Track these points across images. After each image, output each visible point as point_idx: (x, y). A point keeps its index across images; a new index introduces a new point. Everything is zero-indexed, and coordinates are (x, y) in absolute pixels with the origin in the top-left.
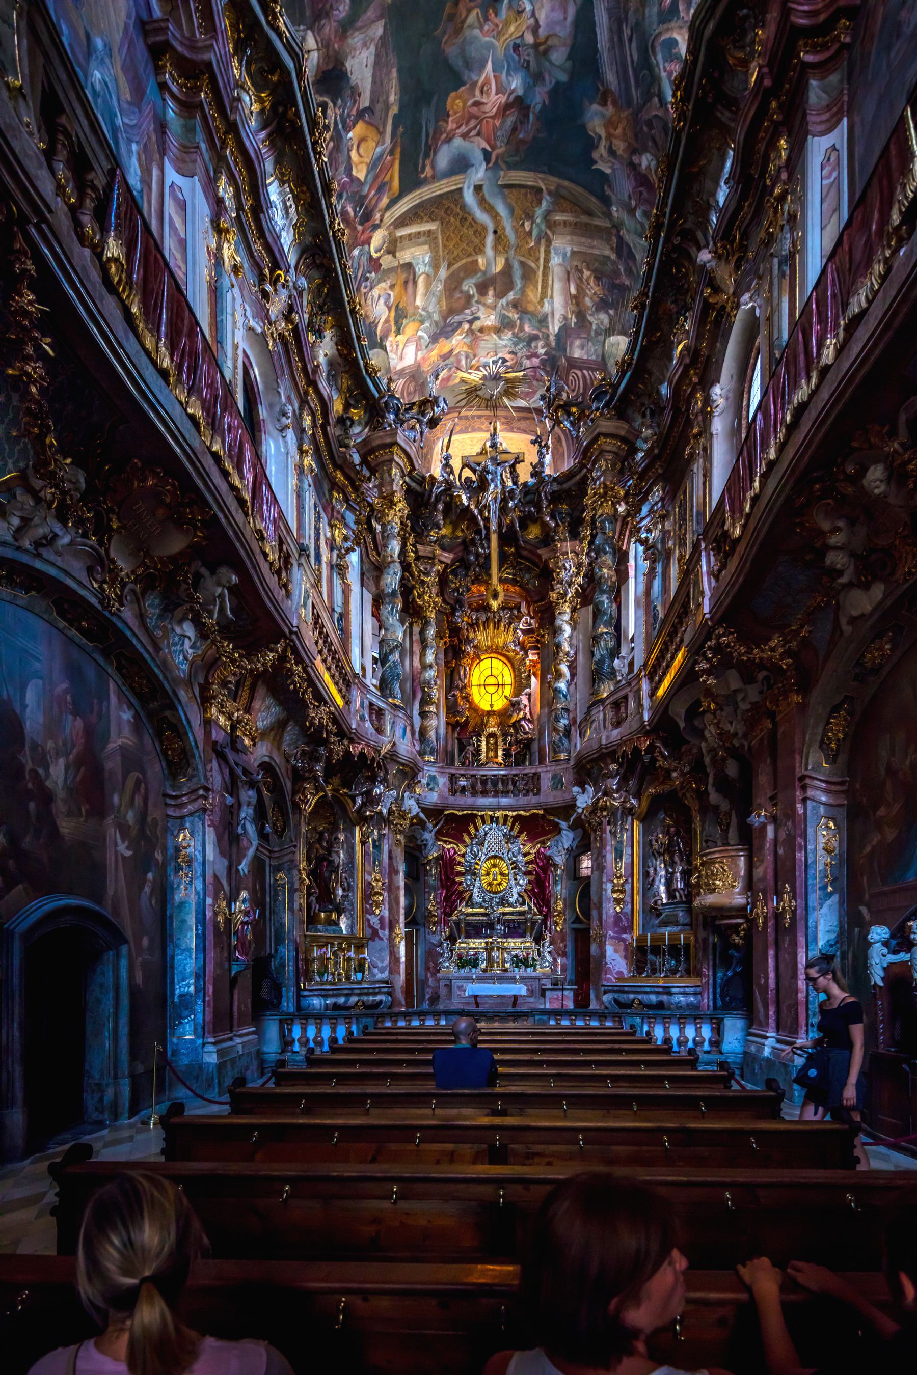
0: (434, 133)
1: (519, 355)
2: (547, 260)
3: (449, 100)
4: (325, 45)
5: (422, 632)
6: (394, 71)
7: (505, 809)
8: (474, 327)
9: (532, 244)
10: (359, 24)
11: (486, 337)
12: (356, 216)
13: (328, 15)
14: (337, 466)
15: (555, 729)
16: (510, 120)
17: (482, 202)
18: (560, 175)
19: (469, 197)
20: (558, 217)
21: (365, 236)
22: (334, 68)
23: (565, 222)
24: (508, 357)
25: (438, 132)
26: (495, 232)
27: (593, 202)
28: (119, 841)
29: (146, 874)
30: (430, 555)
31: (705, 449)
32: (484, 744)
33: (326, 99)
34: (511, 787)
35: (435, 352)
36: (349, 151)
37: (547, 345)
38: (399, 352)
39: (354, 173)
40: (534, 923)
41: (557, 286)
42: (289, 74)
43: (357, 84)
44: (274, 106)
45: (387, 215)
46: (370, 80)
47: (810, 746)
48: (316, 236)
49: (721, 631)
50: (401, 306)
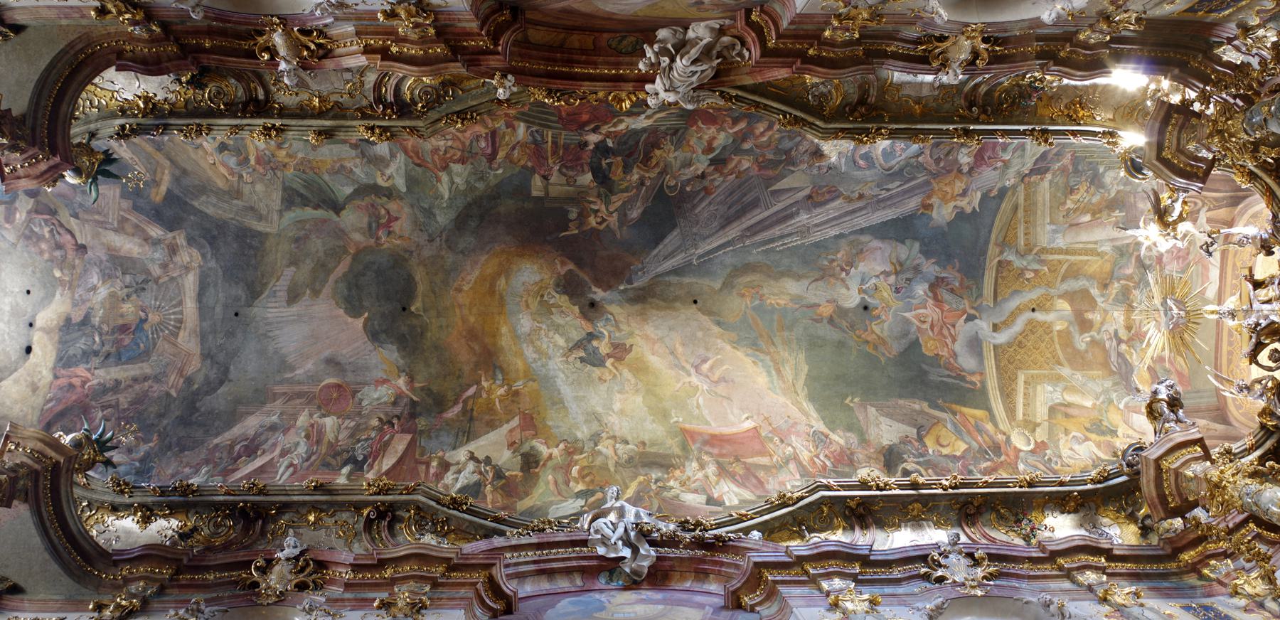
45: (1001, 427)
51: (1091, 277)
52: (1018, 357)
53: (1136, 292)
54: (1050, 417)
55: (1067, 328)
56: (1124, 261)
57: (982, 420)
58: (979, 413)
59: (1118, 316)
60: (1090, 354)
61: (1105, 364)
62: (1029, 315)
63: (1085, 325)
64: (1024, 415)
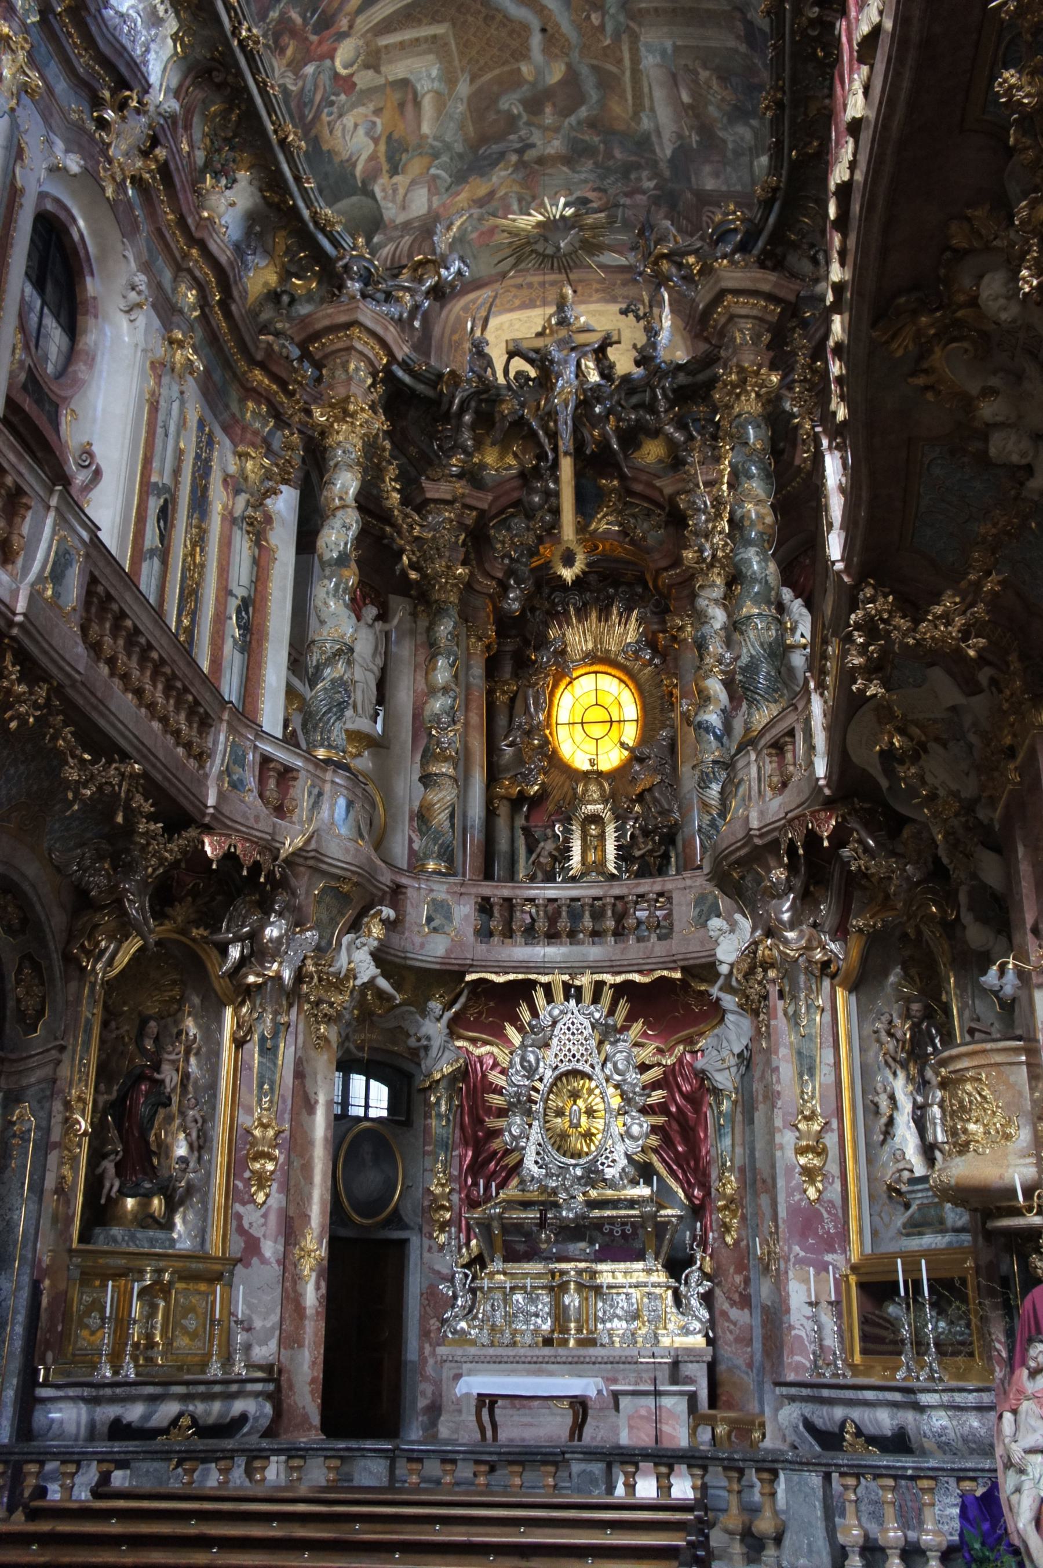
51: (602, 104)
52: (470, 19)
53: (590, 164)
55: (527, 81)
59: (556, 146)
60: (494, 117)
61: (484, 139)
62: (535, 24)
63: (534, 105)
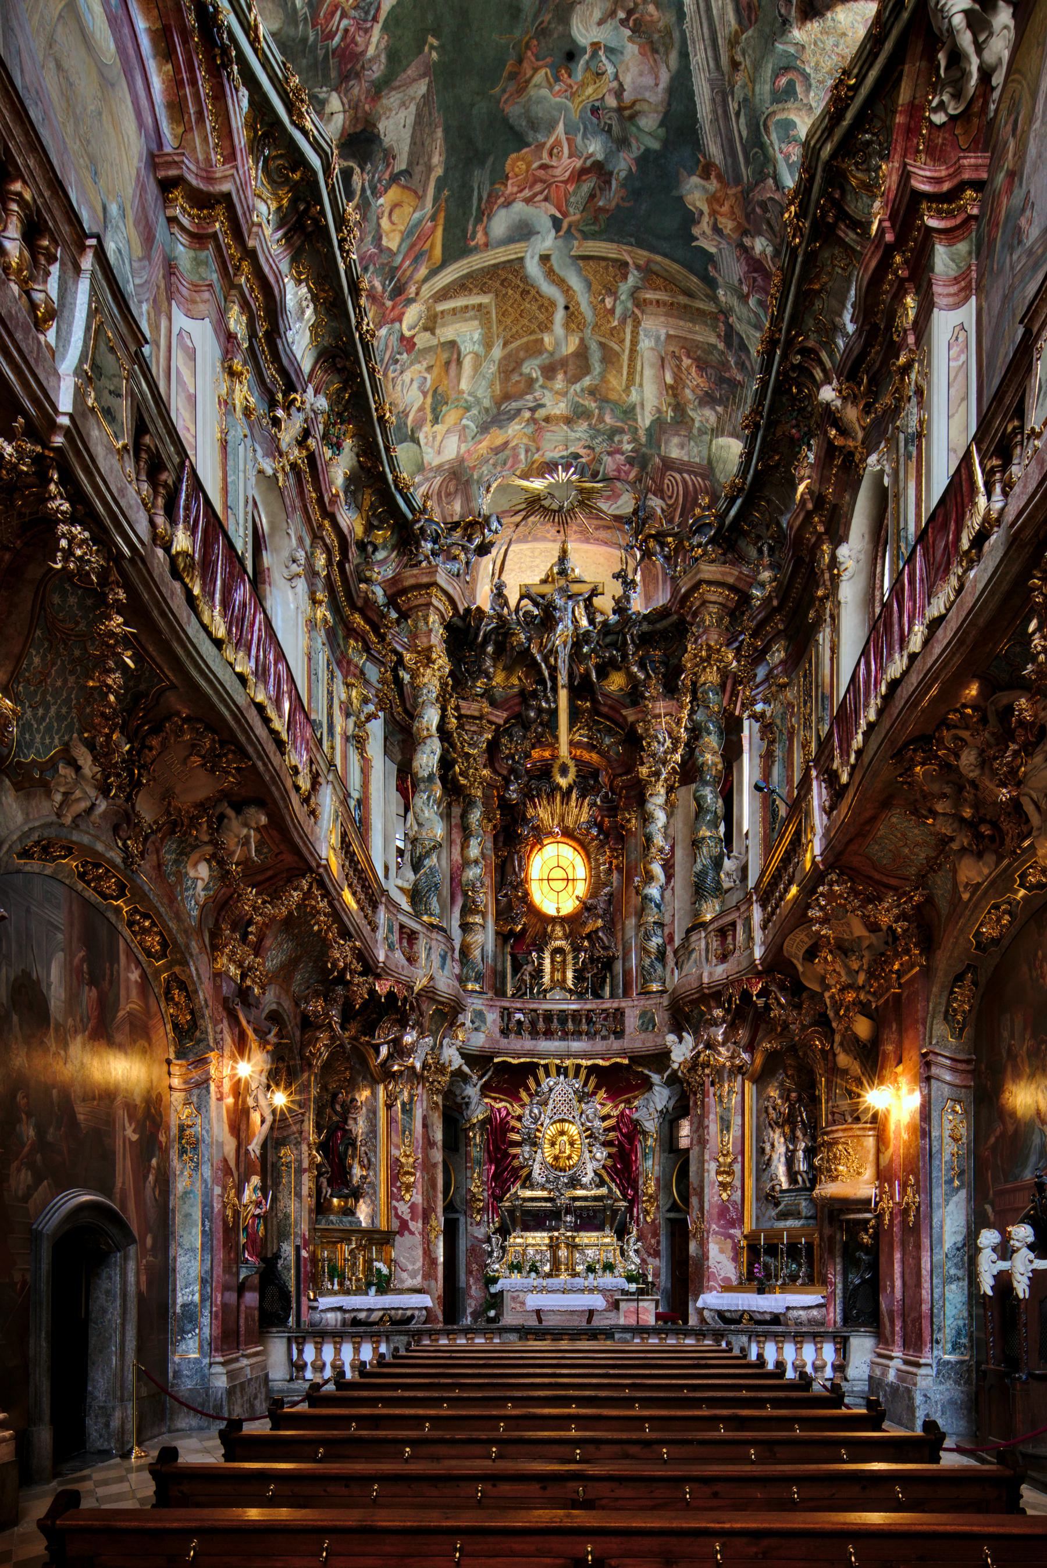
0: (490, 196)
1: (598, 450)
2: (634, 343)
3: (509, 161)
4: (353, 107)
5: (464, 816)
6: (439, 133)
7: (576, 1057)
8: (537, 416)
9: (616, 323)
10: (397, 83)
11: (553, 428)
12: (384, 291)
13: (358, 76)
14: (354, 607)
15: (647, 952)
16: (586, 187)
17: (550, 274)
18: (652, 249)
19: (533, 268)
20: (649, 295)
21: (396, 312)
22: (364, 131)
23: (658, 302)
24: (582, 452)
25: (492, 197)
26: (567, 308)
27: (694, 282)
28: (127, 1124)
29: (150, 1161)
30: (477, 714)
31: (832, 617)
32: (547, 962)
33: (351, 164)
34: (584, 1027)
35: (484, 444)
36: (378, 218)
37: (635, 440)
38: (437, 444)
39: (384, 242)
40: (615, 1212)
41: (648, 373)
42: (314, 173)
43: (391, 148)
44: (293, 202)
46: (408, 141)
47: (933, 1017)
48: (338, 337)
49: (834, 877)
50: (440, 390)
54: (443, 345)
56: (617, 412)
57: (429, 259)
58: (438, 252)
64: (442, 312)
